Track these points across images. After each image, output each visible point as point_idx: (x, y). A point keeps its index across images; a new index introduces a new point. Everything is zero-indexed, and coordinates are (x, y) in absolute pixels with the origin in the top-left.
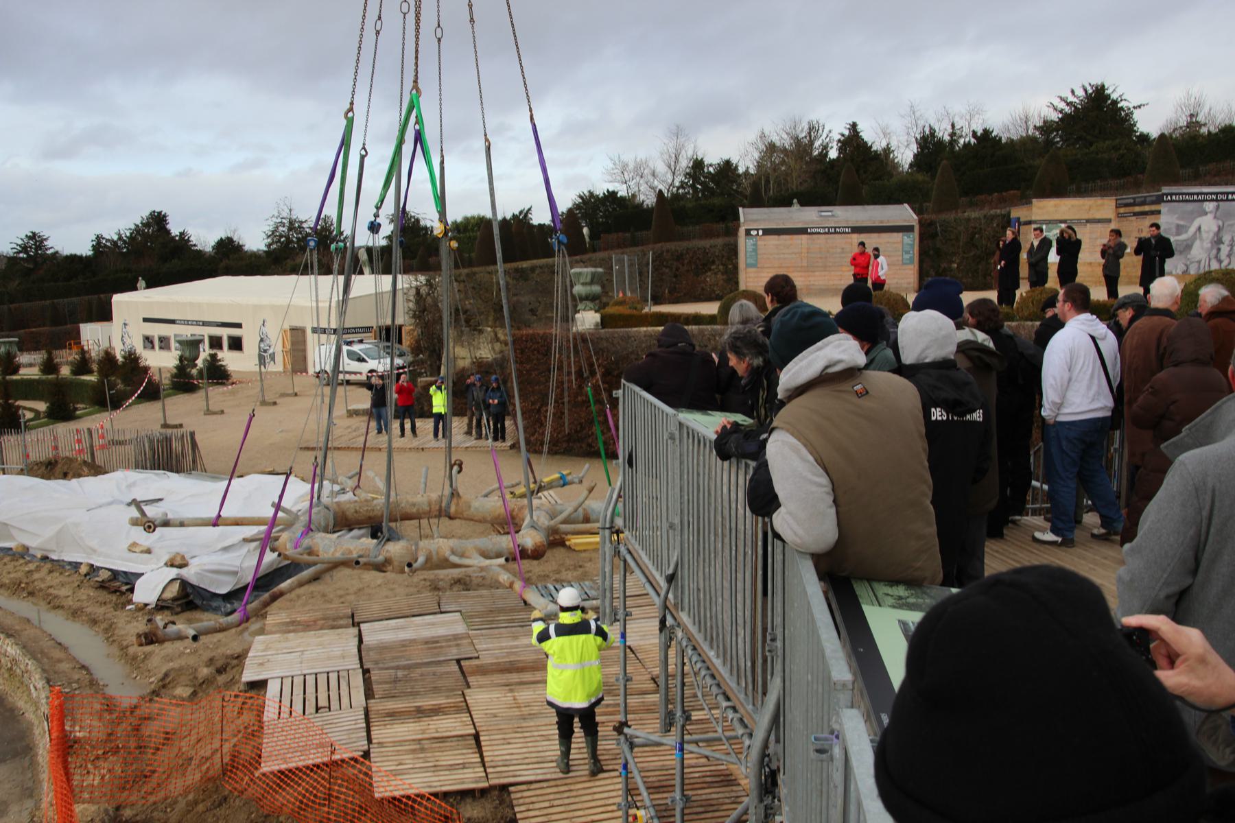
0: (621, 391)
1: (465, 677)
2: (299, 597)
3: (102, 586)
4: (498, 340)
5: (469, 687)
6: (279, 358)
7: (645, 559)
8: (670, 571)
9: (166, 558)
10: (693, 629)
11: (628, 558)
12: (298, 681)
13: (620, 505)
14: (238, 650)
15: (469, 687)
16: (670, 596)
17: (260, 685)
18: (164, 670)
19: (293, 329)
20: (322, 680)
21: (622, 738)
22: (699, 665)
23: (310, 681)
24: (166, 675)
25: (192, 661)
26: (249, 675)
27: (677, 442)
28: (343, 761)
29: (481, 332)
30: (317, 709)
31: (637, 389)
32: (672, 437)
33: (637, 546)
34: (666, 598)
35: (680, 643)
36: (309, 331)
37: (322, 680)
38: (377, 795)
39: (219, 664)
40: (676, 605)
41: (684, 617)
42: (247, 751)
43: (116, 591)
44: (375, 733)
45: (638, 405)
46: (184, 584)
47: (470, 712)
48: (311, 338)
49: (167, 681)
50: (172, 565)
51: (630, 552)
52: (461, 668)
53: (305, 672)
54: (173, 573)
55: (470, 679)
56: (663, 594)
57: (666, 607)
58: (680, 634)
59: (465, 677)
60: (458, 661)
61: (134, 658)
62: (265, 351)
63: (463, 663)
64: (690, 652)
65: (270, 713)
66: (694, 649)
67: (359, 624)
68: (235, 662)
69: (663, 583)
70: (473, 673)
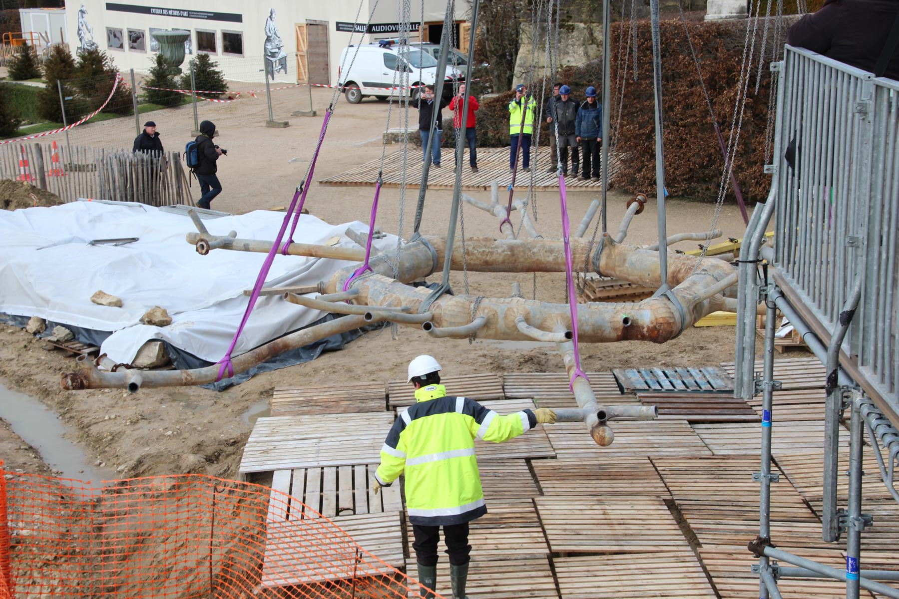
0: (782, 63)
1: (537, 482)
2: (316, 371)
3: (57, 347)
4: (593, 40)
5: (542, 494)
6: (292, 63)
7: (807, 300)
8: (848, 308)
9: (142, 312)
10: (882, 389)
11: (780, 303)
12: (313, 475)
13: (770, 233)
14: (235, 434)
15: (542, 494)
16: (845, 346)
17: (262, 478)
18: (137, 456)
19: (311, 24)
20: (345, 474)
22: (888, 439)
23: (330, 475)
24: (140, 462)
25: (173, 446)
26: (249, 465)
27: (871, 117)
29: (572, 28)
30: (338, 511)
31: (809, 54)
32: (863, 112)
33: (794, 284)
34: (839, 347)
35: (858, 412)
36: (332, 27)
37: (345, 474)
39: (209, 451)
40: (853, 359)
41: (866, 373)
42: (243, 561)
43: (75, 355)
45: (809, 77)
46: (166, 346)
47: (542, 526)
48: (336, 39)
49: (141, 469)
50: (150, 322)
51: (782, 294)
52: (531, 469)
54: (152, 331)
55: (543, 484)
56: (832, 344)
57: (838, 365)
58: (857, 398)
59: (537, 482)
60: (528, 460)
61: (98, 440)
62: (273, 55)
63: (534, 463)
64: (874, 421)
65: (276, 512)
66: (881, 417)
67: (395, 407)
68: (230, 449)
69: (834, 329)
70: (548, 477)
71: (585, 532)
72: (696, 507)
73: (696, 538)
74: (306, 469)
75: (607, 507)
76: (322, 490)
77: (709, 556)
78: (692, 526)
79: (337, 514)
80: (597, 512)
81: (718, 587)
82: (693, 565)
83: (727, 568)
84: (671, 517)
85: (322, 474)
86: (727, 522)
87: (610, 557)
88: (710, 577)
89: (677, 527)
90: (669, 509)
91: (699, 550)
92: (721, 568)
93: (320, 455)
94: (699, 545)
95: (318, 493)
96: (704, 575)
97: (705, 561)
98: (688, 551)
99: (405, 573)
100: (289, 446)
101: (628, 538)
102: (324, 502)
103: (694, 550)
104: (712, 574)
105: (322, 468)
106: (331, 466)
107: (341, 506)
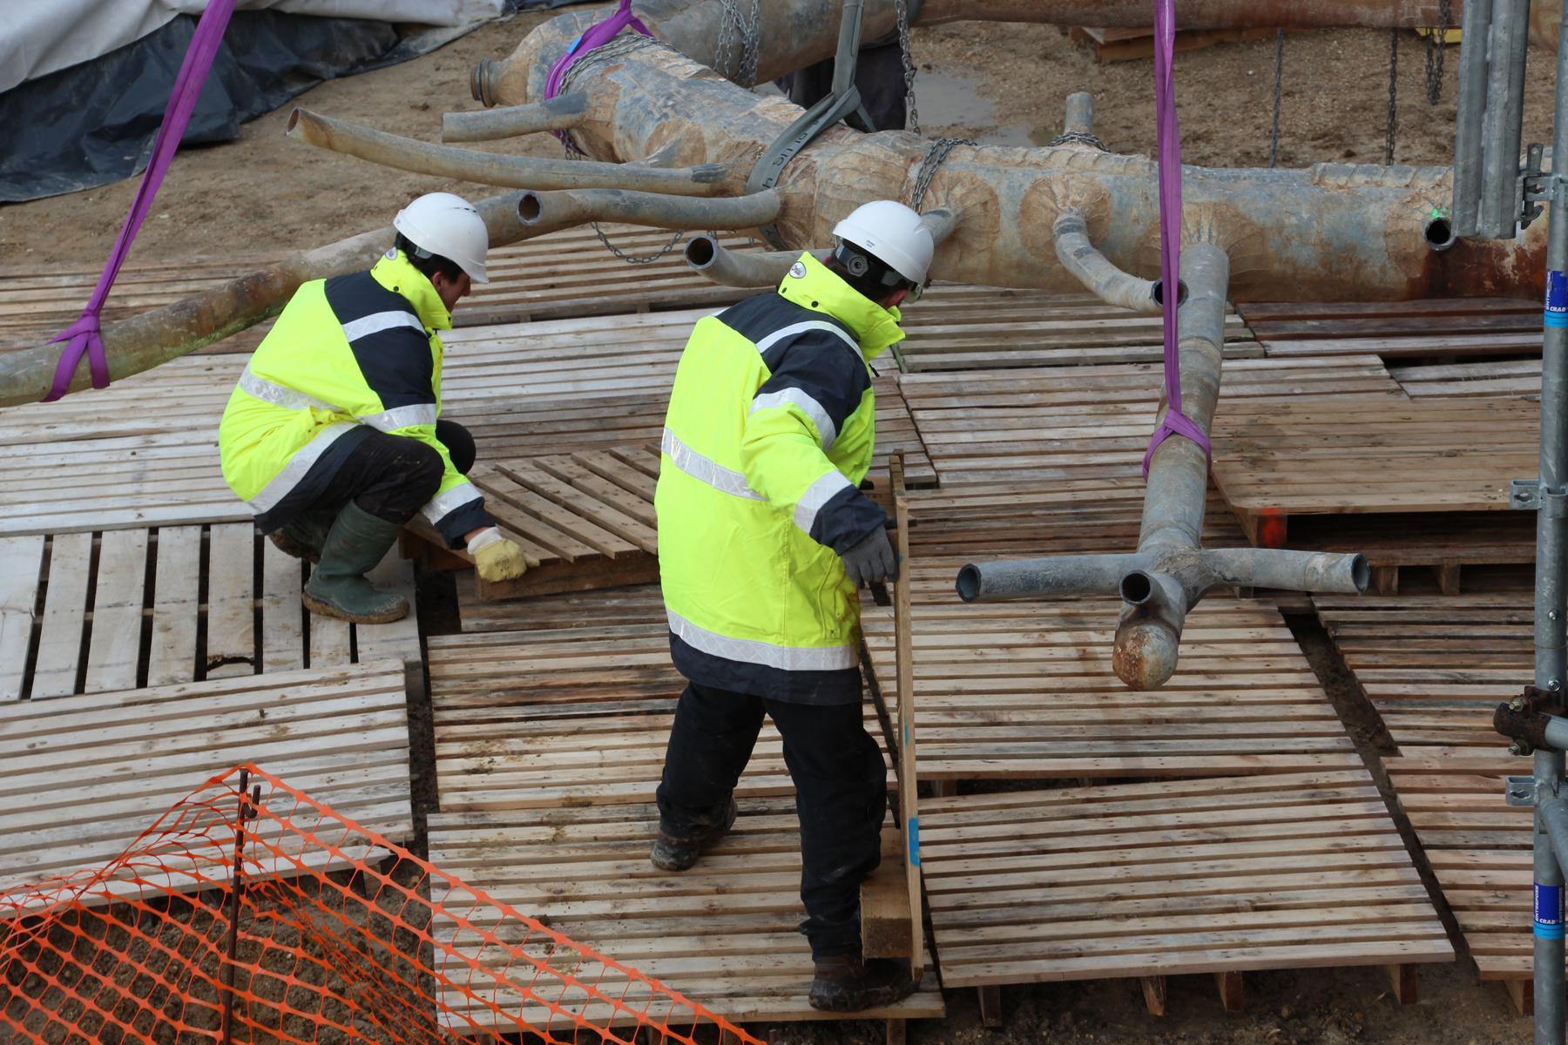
12: (123, 552)
21: (1540, 766)
23: (178, 552)
28: (307, 881)
30: (203, 666)
38: (445, 1021)
44: (450, 772)
53: (153, 515)
71: (1016, 717)
72: (1388, 631)
73: (1382, 730)
74: (97, 534)
75: (1094, 637)
76: (149, 601)
77: (1419, 781)
78: (1370, 689)
79: (200, 676)
80: (1058, 652)
81: (1443, 876)
82: (1364, 810)
83: (1477, 819)
84: (1303, 663)
85: (152, 549)
86: (1487, 674)
87: (1095, 793)
88: (1416, 849)
89: (1319, 693)
90: (1299, 637)
91: (1388, 763)
92: (1457, 820)
93: (148, 487)
94: (1391, 749)
95: (135, 611)
96: (1397, 840)
97: (1405, 799)
98: (1351, 769)
99: (425, 856)
100: (38, 462)
101: (1156, 730)
102: (157, 638)
103: (1371, 763)
104: (1424, 837)
105: (154, 530)
106: (182, 524)
107: (215, 648)
